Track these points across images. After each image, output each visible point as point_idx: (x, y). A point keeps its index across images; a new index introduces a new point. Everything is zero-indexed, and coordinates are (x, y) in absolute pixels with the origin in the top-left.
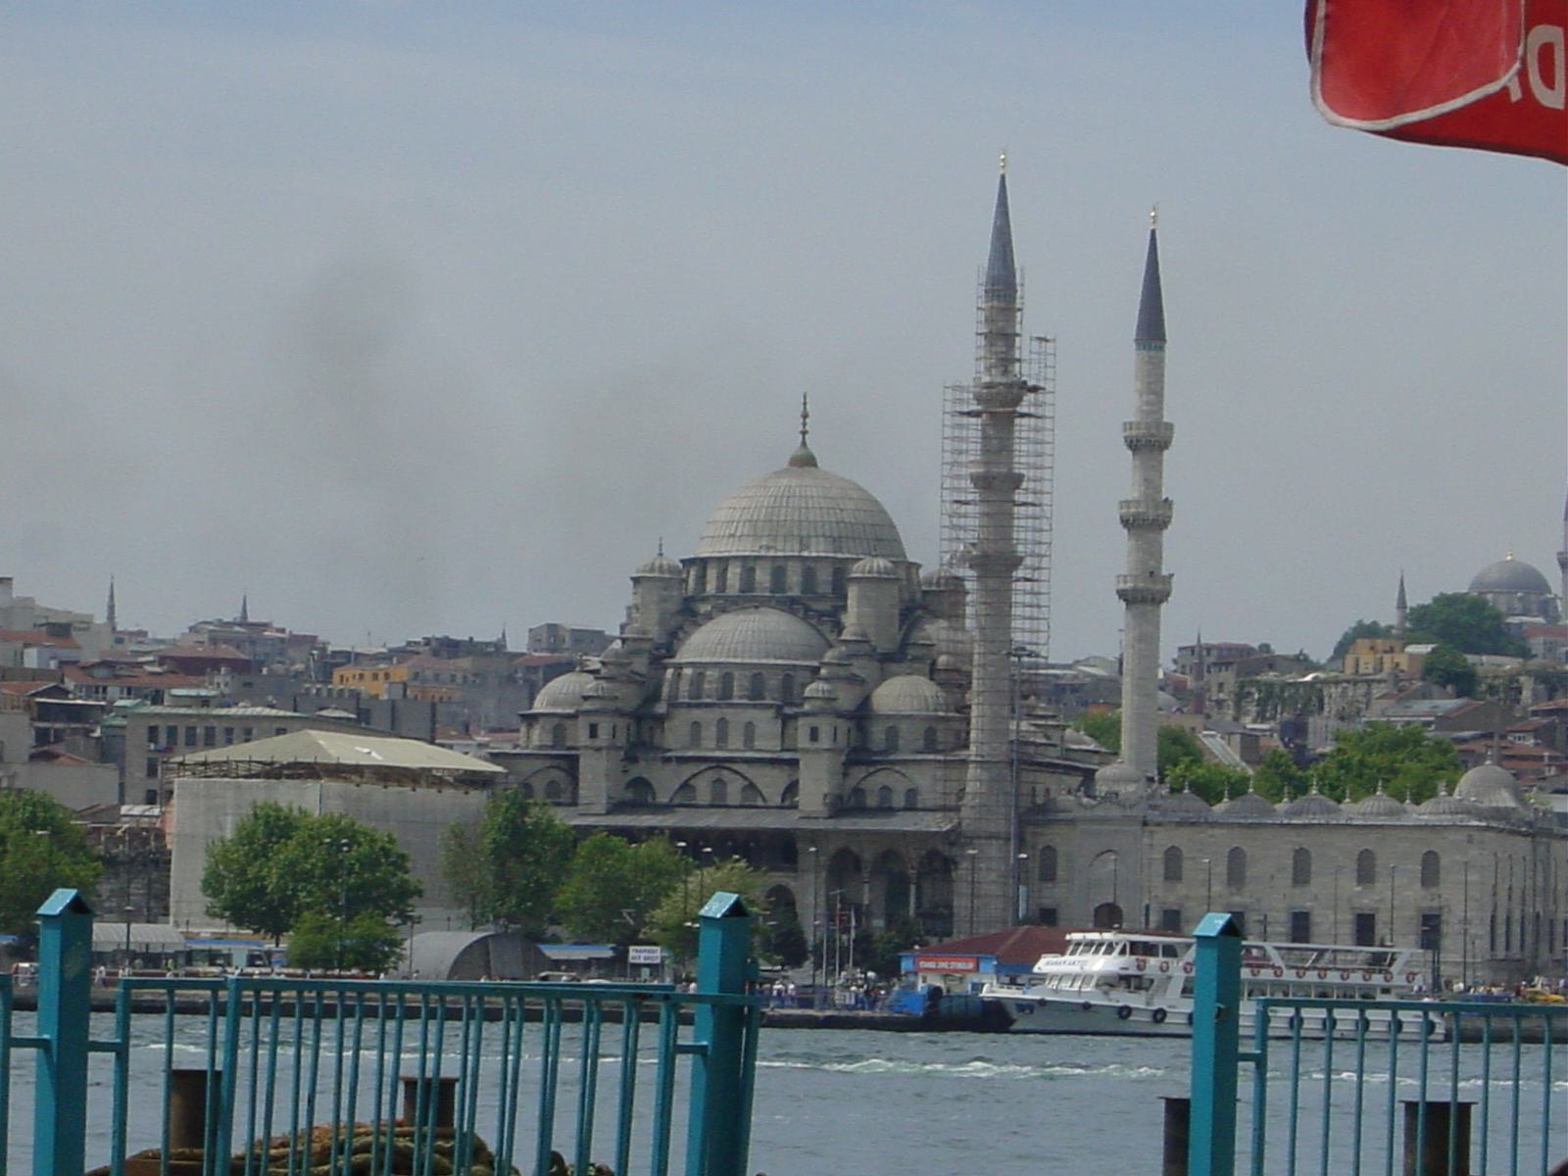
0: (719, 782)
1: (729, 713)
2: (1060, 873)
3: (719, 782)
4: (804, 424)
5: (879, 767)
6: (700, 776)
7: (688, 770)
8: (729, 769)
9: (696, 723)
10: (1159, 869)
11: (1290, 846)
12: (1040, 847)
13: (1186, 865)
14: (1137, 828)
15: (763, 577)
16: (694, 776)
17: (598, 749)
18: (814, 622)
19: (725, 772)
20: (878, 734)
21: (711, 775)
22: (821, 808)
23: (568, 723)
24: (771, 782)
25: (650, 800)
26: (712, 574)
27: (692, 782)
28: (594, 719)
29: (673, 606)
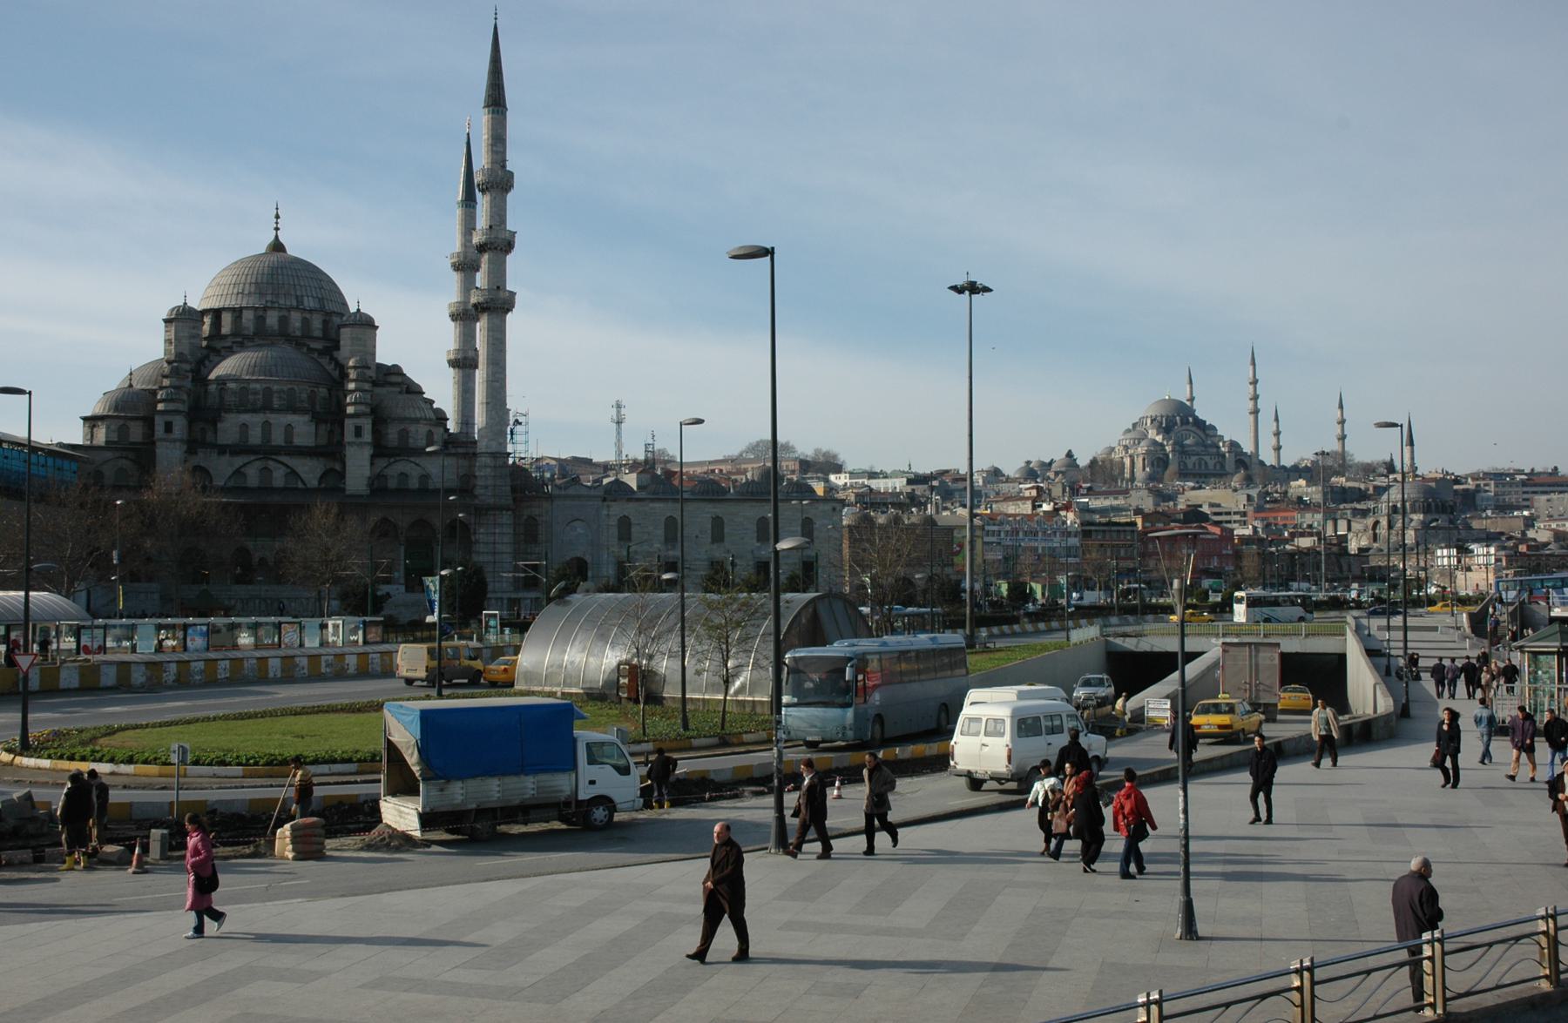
0: (266, 471)
3: (266, 471)
4: (277, 223)
7: (239, 461)
8: (273, 460)
9: (244, 424)
10: (614, 531)
11: (709, 516)
12: (525, 517)
14: (600, 503)
16: (245, 465)
17: (175, 441)
19: (271, 464)
21: (259, 464)
22: (365, 488)
24: (310, 471)
26: (227, 319)
27: (242, 470)
28: (169, 418)
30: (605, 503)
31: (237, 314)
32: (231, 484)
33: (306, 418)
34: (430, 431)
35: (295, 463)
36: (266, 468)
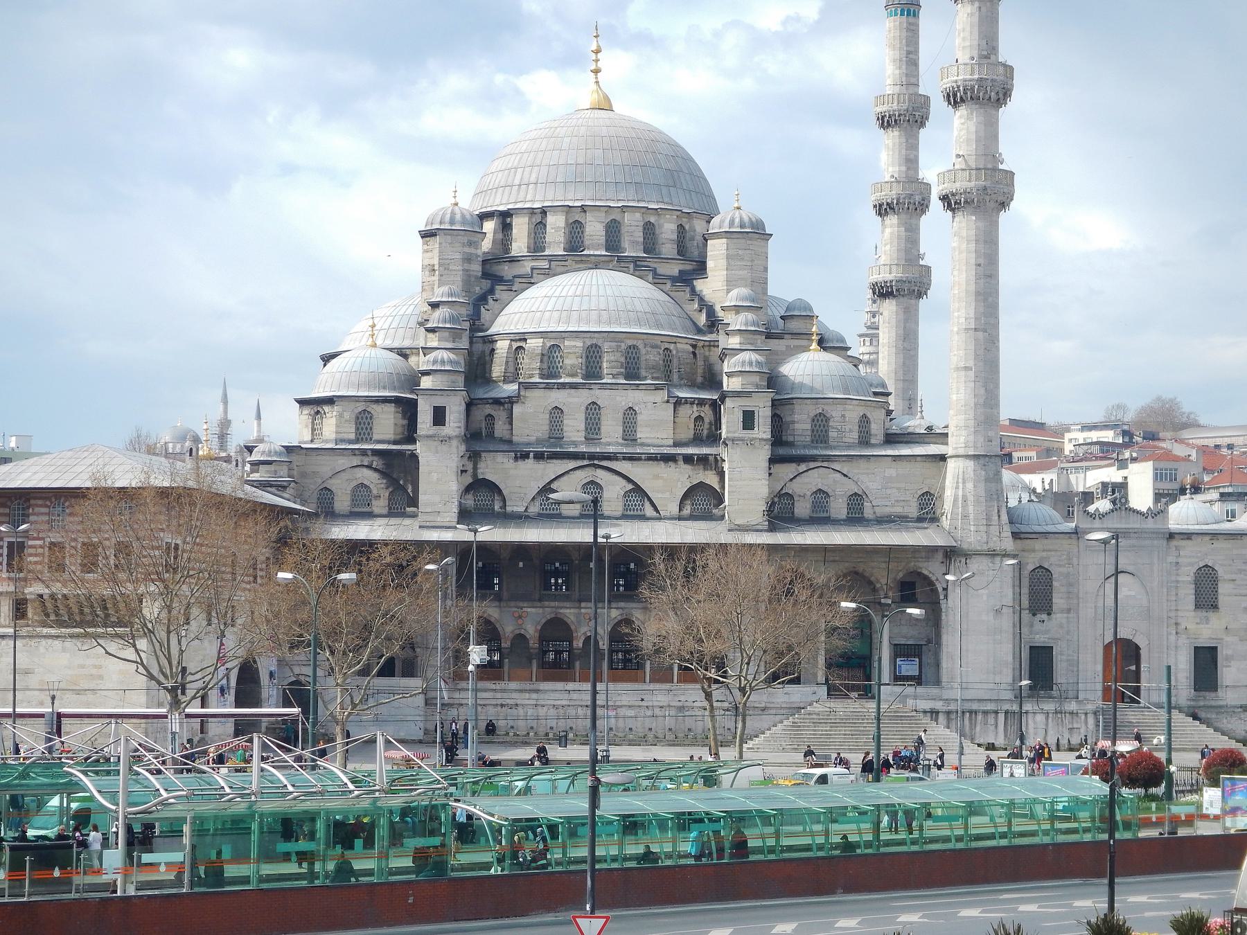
1: (602, 397)
2: (1058, 601)
4: (597, 61)
5: (812, 465)
6: (565, 478)
12: (1031, 567)
13: (1223, 589)
14: (1165, 542)
15: (594, 229)
18: (668, 286)
19: (600, 473)
20: (801, 423)
23: (376, 409)
25: (497, 508)
26: (521, 229)
29: (477, 268)
30: (1174, 543)
31: (538, 218)
32: (535, 509)
33: (663, 395)
34: (864, 416)
35: (641, 473)
36: (592, 482)
